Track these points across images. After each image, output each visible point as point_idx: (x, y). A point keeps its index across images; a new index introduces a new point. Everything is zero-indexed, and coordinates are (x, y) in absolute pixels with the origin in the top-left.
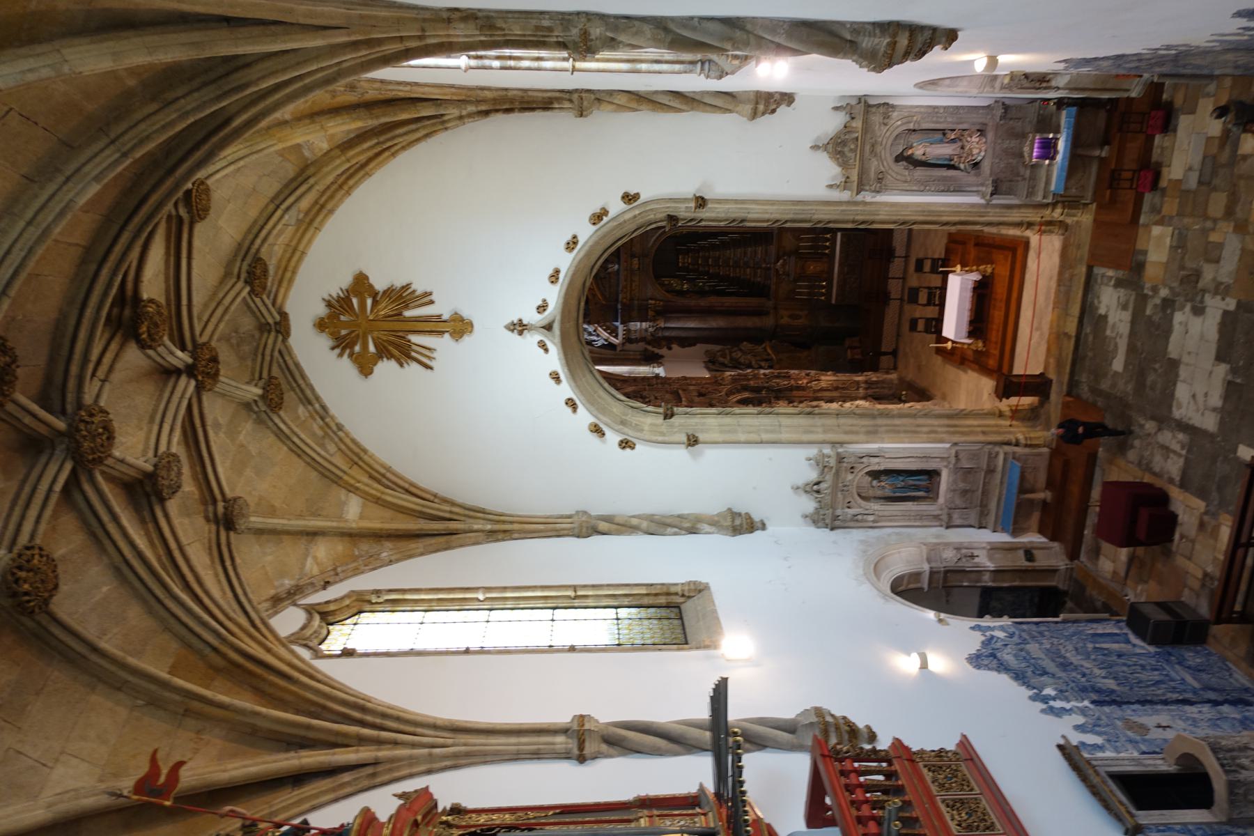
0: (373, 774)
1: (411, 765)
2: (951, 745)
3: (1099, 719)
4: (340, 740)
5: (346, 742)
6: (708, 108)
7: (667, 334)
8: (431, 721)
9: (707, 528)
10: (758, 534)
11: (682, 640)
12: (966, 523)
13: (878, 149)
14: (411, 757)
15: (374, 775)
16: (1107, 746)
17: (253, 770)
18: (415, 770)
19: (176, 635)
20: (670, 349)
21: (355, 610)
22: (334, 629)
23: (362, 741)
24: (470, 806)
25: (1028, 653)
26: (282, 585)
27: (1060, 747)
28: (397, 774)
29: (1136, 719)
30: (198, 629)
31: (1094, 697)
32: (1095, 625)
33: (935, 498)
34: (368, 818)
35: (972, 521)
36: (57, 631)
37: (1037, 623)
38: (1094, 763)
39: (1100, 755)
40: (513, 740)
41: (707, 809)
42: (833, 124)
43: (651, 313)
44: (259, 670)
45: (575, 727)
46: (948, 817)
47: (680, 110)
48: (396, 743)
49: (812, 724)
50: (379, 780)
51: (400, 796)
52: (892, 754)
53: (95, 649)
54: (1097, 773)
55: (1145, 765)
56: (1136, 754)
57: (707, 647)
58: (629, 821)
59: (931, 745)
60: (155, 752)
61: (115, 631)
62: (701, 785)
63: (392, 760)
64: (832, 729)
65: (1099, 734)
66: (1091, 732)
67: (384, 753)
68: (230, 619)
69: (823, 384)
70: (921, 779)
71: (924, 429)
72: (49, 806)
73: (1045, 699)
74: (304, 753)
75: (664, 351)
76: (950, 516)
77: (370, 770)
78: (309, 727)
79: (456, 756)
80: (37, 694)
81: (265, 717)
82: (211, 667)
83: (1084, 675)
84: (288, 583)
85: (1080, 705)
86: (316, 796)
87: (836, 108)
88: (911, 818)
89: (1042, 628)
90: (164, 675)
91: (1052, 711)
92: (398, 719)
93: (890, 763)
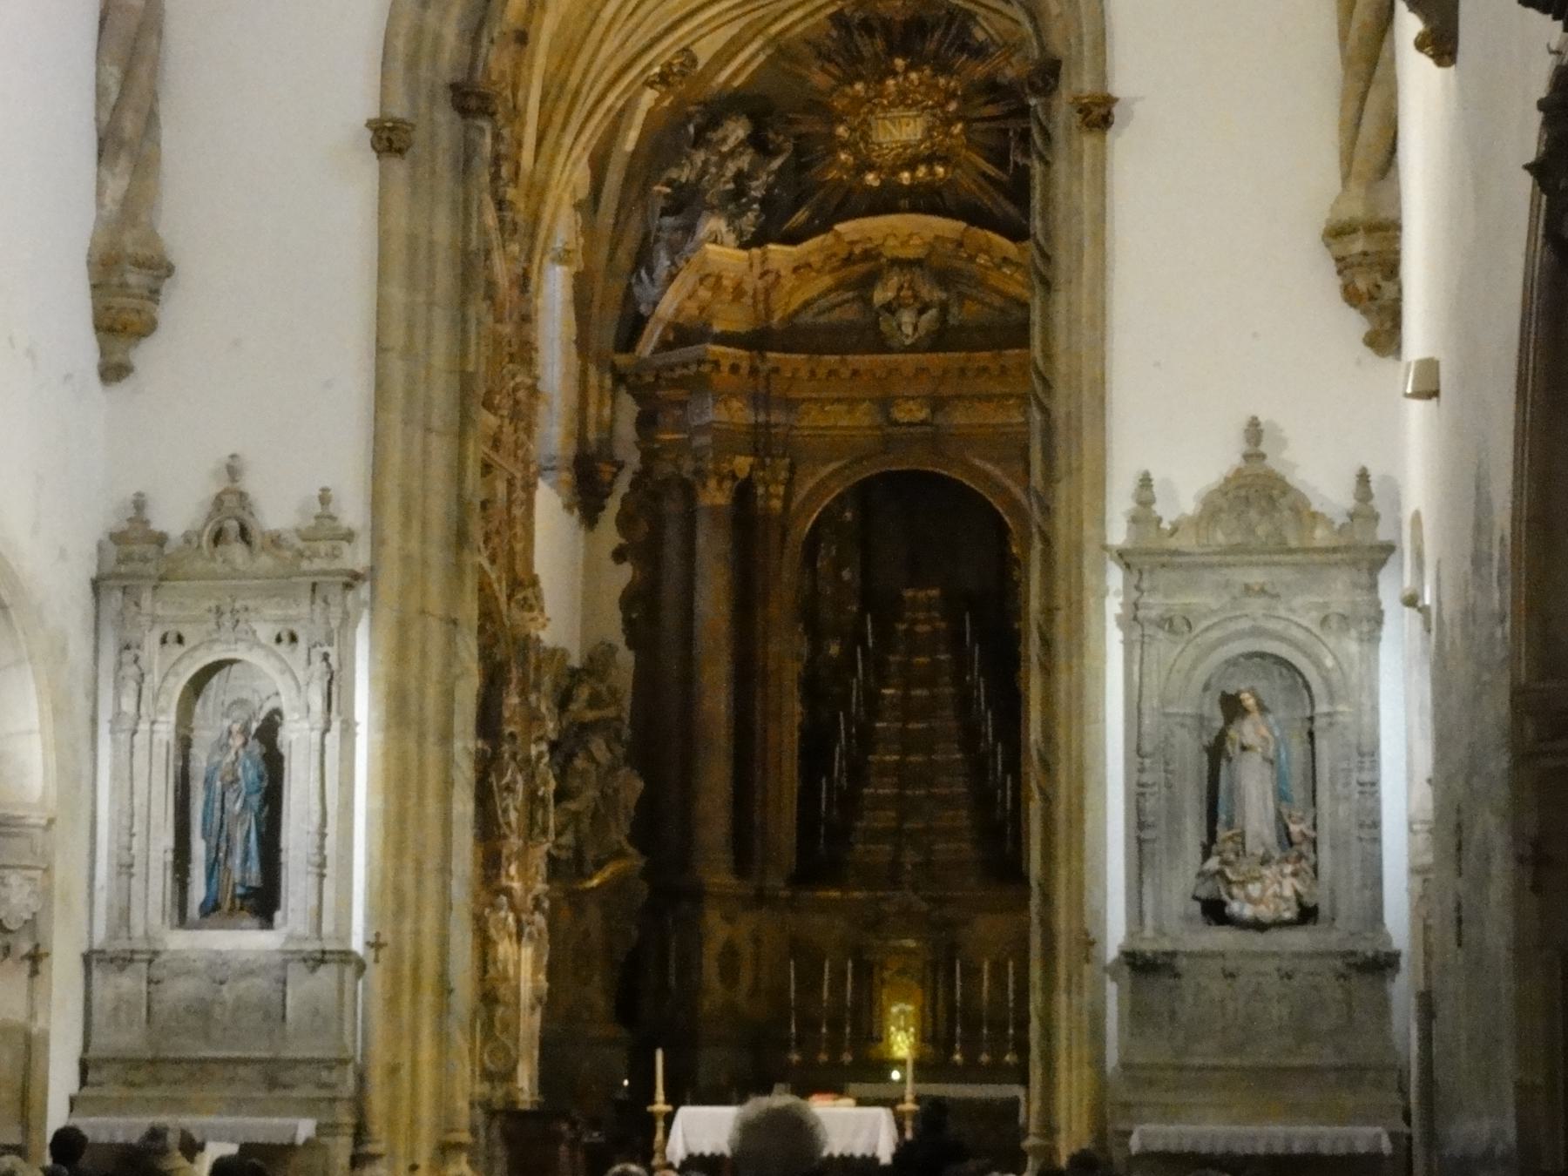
6: (1353, 105)
7: (672, 532)
9: (117, 186)
10: (84, 348)
12: (97, 1018)
13: (1256, 606)
20: (619, 555)
33: (182, 920)
35: (110, 1040)
42: (1322, 480)
43: (743, 464)
47: (1343, 37)
69: (505, 948)
71: (409, 879)
75: (609, 534)
76: (123, 961)
87: (1363, 477)
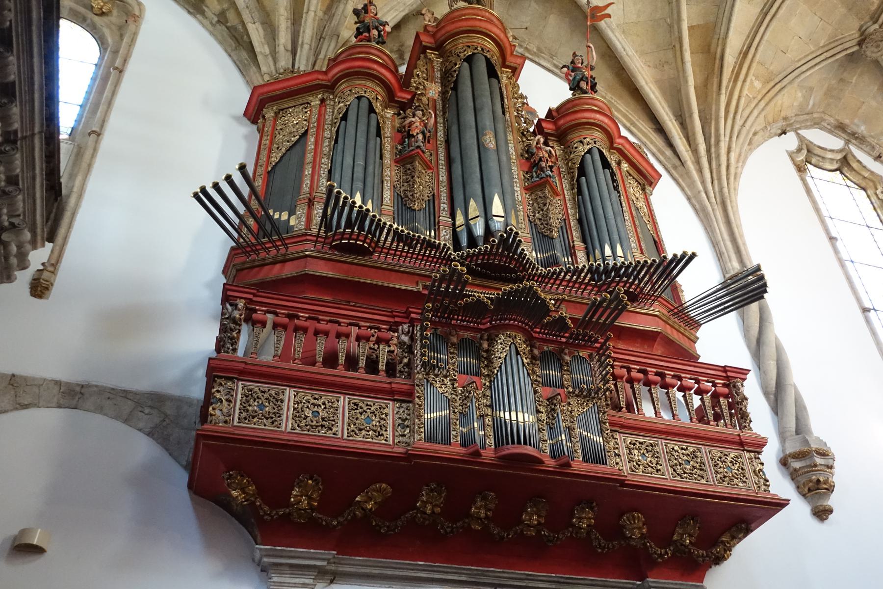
1: (688, 186)
15: (675, 168)
17: (652, 96)
18: (686, 189)
21: (863, 184)
23: (695, 151)
24: (653, 199)
26: (858, 126)
28: (680, 180)
40: (726, 237)
48: (700, 171)
50: (673, 171)
63: (688, 173)
64: (808, 462)
67: (690, 165)
77: (678, 163)
78: (691, 115)
84: (862, 129)
86: (652, 142)
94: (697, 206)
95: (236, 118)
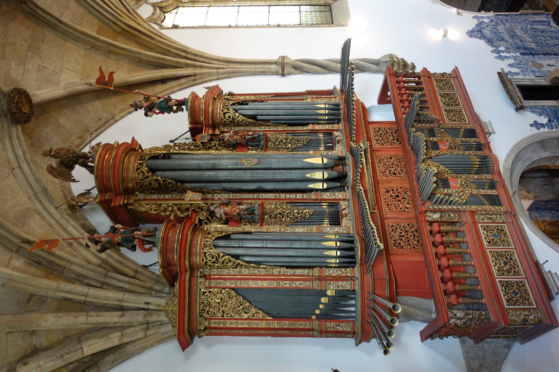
0: (194, 79)
1: (210, 76)
2: (449, 71)
3: (521, 61)
4: (178, 65)
5: (180, 66)
8: (217, 58)
11: (331, 22)
14: (209, 73)
15: (195, 80)
16: (521, 73)
18: (211, 78)
19: (95, 16)
21: (175, 6)
22: (167, 15)
23: (187, 66)
24: (236, 93)
25: (497, 30)
27: (499, 73)
28: (204, 80)
29: (540, 62)
30: (104, 13)
31: (523, 51)
32: (535, 17)
34: (194, 96)
36: (40, 12)
37: (506, 15)
38: (512, 80)
39: (516, 77)
40: (253, 66)
41: (336, 96)
44: (136, 33)
45: (280, 61)
46: (440, 101)
48: (202, 67)
49: (387, 61)
50: (197, 82)
51: (207, 88)
52: (421, 74)
53: (61, 22)
54: (512, 85)
55: (535, 82)
56: (533, 77)
57: (342, 26)
58: (303, 99)
59: (440, 71)
60: (101, 68)
61: (67, 13)
62: (334, 86)
63: (202, 74)
65: (519, 68)
66: (516, 67)
67: (198, 71)
68: (118, 9)
70: (432, 85)
72: (64, 89)
73: (498, 52)
74: (163, 70)
77: (193, 78)
78: (163, 59)
79: (228, 73)
80: (43, 41)
81: (144, 54)
82: (115, 31)
83: (521, 41)
85: (514, 55)
88: (424, 101)
89: (509, 17)
90: (95, 35)
91: (501, 58)
92: (202, 56)
93: (419, 78)
94: (225, 76)
95: (187, 358)
